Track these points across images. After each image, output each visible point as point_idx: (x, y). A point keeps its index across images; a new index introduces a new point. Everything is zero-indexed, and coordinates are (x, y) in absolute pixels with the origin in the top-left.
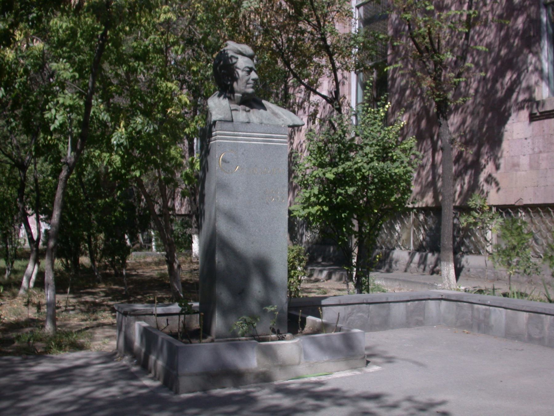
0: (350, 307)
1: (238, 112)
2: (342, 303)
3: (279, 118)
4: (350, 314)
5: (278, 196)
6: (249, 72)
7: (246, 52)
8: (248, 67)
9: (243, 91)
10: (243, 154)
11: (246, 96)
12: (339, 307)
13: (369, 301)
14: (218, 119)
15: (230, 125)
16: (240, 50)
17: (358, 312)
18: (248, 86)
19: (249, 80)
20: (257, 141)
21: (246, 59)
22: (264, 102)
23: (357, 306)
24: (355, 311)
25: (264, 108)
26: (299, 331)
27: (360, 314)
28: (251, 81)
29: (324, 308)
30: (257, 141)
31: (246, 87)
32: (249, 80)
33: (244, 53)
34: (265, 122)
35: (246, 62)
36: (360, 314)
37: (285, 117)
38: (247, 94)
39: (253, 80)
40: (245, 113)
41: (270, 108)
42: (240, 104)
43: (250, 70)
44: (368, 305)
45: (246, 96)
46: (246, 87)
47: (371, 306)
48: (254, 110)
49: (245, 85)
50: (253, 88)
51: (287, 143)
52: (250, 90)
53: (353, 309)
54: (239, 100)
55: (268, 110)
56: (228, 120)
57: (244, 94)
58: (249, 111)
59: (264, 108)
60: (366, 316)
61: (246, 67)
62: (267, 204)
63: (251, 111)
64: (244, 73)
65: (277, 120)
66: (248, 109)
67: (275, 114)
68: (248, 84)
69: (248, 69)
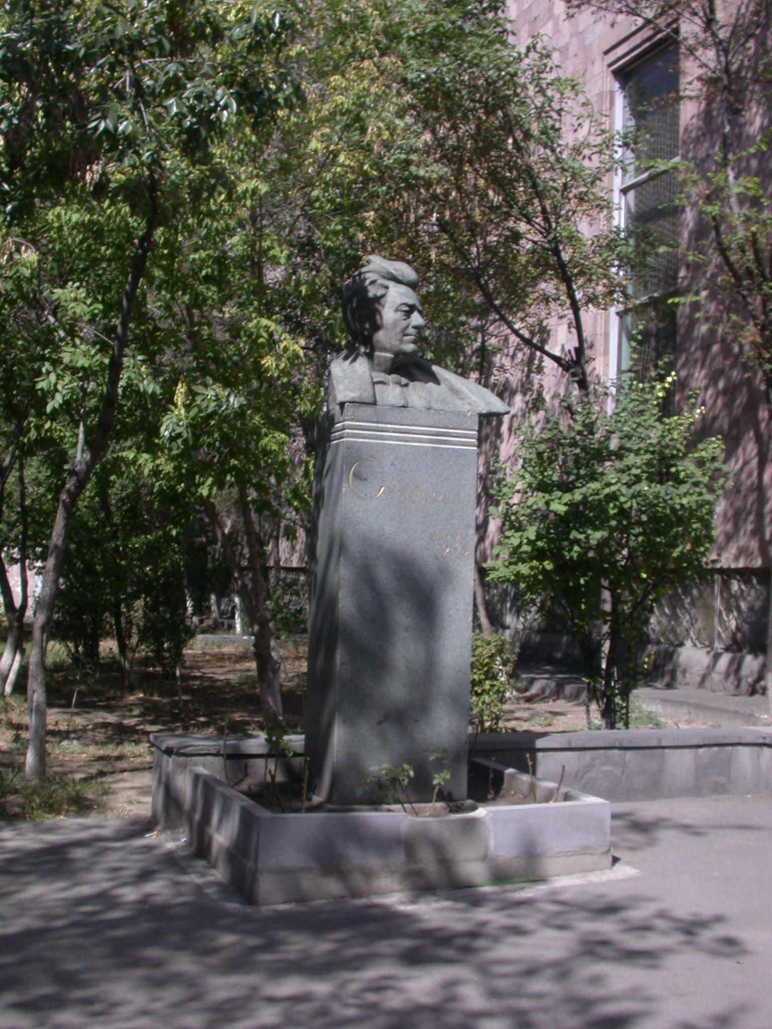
0: (588, 754)
1: (385, 387)
2: (573, 746)
3: (462, 399)
4: (589, 767)
6: (408, 314)
7: (403, 276)
10: (392, 464)
11: (401, 357)
12: (568, 753)
13: (625, 744)
14: (347, 399)
15: (369, 410)
16: (393, 272)
17: (603, 764)
18: (406, 338)
19: (407, 327)
20: (420, 441)
21: (403, 289)
22: (435, 368)
23: (602, 751)
24: (597, 762)
25: (434, 379)
26: (490, 797)
27: (607, 768)
28: (411, 330)
29: (540, 755)
30: (420, 441)
31: (401, 341)
32: (407, 327)
34: (436, 406)
35: (402, 295)
36: (607, 768)
37: (473, 398)
38: (405, 353)
39: (415, 327)
40: (398, 389)
41: (446, 380)
42: (390, 372)
43: (411, 309)
44: (622, 752)
45: (401, 357)
46: (401, 341)
47: (629, 754)
49: (399, 337)
50: (414, 342)
52: (410, 347)
53: (593, 759)
54: (389, 364)
55: (443, 385)
57: (398, 354)
58: (406, 385)
59: (434, 379)
60: (618, 772)
63: (411, 384)
64: (399, 315)
65: (459, 402)
66: (404, 381)
67: (454, 391)
69: (406, 309)
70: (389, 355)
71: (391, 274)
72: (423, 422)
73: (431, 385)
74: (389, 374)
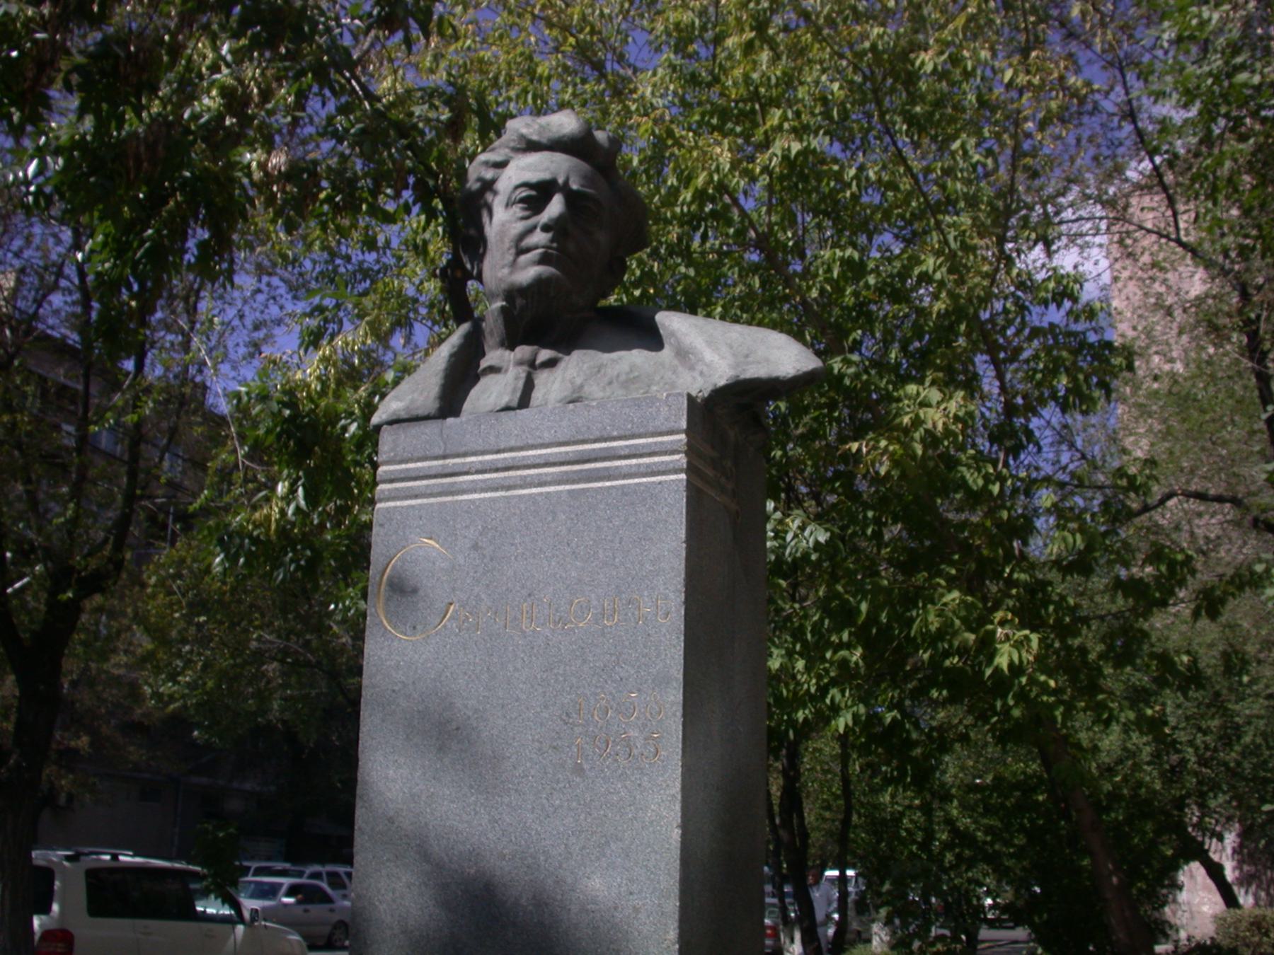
3: (692, 368)
5: (634, 733)
8: (526, 185)
9: (503, 286)
10: (475, 547)
11: (519, 302)
16: (524, 131)
28: (539, 237)
33: (535, 138)
41: (673, 334)
48: (577, 354)
50: (543, 260)
51: (676, 471)
55: (666, 353)
56: (421, 412)
58: (551, 364)
61: (517, 187)
62: (579, 770)
64: (517, 210)
66: (545, 354)
67: (683, 354)
68: (521, 251)
70: (499, 303)
71: (522, 137)
72: (547, 437)
73: (637, 358)
74: (512, 348)
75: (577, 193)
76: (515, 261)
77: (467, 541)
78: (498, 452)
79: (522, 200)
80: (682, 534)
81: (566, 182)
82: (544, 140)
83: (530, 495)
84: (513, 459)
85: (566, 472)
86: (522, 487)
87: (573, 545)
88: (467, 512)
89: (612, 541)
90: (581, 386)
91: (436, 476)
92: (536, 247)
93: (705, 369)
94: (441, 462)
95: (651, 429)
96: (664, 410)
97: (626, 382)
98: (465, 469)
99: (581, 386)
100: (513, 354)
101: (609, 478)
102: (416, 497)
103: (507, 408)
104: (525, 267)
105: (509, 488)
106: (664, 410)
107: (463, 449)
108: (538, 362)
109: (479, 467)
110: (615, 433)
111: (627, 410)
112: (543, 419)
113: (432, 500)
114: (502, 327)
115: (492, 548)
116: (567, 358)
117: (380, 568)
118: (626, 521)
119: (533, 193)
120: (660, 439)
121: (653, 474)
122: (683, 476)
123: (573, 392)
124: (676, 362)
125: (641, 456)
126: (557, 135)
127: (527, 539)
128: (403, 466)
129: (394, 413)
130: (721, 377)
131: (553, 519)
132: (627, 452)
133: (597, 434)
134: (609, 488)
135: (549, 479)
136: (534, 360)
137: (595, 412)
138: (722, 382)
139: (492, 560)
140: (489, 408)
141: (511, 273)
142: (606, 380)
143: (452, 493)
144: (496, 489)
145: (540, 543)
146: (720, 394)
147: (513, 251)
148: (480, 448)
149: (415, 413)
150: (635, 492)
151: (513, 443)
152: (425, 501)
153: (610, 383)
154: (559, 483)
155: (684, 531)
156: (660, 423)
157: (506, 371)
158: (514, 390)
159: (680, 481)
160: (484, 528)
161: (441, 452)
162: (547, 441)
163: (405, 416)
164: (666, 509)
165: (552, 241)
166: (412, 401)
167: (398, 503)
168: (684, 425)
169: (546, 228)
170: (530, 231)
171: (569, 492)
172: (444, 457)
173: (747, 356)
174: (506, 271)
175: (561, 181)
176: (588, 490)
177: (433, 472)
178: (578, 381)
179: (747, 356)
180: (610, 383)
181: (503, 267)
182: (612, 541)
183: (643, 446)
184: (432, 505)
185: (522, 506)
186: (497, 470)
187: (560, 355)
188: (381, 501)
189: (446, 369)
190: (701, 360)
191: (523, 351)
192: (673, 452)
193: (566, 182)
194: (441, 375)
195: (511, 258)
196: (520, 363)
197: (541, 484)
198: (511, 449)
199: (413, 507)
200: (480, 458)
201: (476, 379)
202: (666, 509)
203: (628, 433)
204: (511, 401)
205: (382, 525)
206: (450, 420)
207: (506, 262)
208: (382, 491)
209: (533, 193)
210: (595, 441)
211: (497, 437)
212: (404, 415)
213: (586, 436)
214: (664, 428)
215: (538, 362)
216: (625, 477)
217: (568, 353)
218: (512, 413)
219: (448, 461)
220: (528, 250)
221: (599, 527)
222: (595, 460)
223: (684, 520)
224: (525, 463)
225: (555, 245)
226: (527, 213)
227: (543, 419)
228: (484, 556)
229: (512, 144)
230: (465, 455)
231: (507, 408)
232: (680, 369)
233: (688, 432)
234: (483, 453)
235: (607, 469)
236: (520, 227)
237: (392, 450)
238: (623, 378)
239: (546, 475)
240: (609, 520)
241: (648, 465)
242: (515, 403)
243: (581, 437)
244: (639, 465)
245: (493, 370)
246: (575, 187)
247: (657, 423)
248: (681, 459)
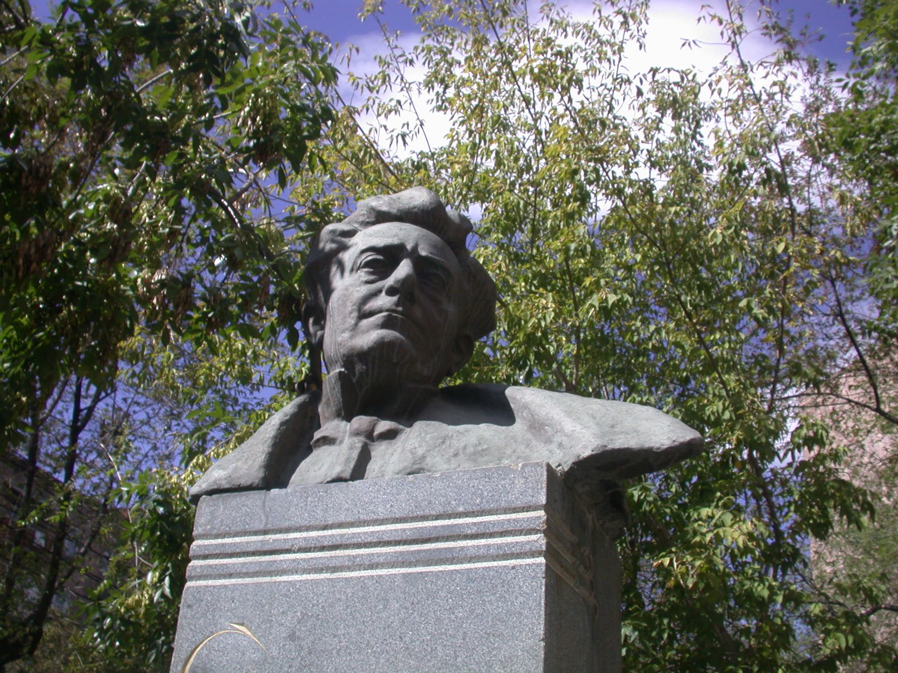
3: (549, 441)
9: (343, 351)
10: (292, 637)
11: (359, 367)
28: (384, 301)
33: (385, 208)
38: (363, 356)
41: (525, 407)
48: (419, 425)
50: (387, 324)
51: (533, 554)
55: (518, 427)
56: (244, 482)
58: (390, 435)
66: (384, 426)
67: (538, 427)
68: (364, 315)
70: (338, 369)
74: (348, 419)
75: (425, 259)
76: (356, 324)
77: (283, 629)
78: (325, 528)
79: (367, 264)
80: (541, 630)
81: (415, 248)
82: (394, 211)
83: (359, 578)
84: (342, 536)
85: (402, 553)
86: (349, 569)
87: (407, 639)
88: (286, 595)
89: (454, 637)
90: (423, 457)
91: (254, 554)
92: (380, 311)
93: (565, 440)
94: (260, 538)
95: (503, 504)
96: (520, 483)
97: (474, 453)
98: (287, 547)
99: (423, 457)
100: (349, 424)
101: (452, 561)
102: (231, 576)
103: (339, 479)
104: (368, 330)
105: (335, 569)
106: (520, 483)
107: (286, 524)
108: (376, 433)
109: (303, 544)
110: (461, 509)
111: (476, 482)
112: (378, 491)
113: (248, 580)
114: (339, 395)
115: (311, 638)
116: (408, 430)
117: (184, 656)
118: (472, 611)
119: (380, 257)
120: (513, 516)
121: (506, 557)
122: (542, 560)
123: (414, 463)
124: (529, 436)
125: (492, 535)
126: (407, 207)
127: (352, 630)
128: (220, 541)
129: (215, 482)
130: (585, 447)
131: (385, 607)
132: (474, 530)
133: (440, 509)
134: (452, 572)
135: (382, 560)
136: (373, 431)
137: (438, 485)
138: (587, 453)
139: (310, 653)
140: (319, 480)
141: (351, 337)
142: (451, 451)
143: (270, 573)
144: (320, 571)
145: (367, 636)
146: (583, 467)
147: (355, 314)
148: (306, 523)
149: (237, 482)
150: (483, 578)
151: (342, 518)
152: (240, 581)
153: (456, 455)
154: (393, 565)
155: (542, 627)
156: (515, 498)
157: (341, 442)
158: (348, 460)
159: (538, 565)
160: (304, 615)
161: (262, 527)
162: (381, 516)
163: (227, 486)
164: (521, 599)
165: (397, 304)
166: (236, 469)
167: (211, 582)
168: (543, 500)
169: (391, 291)
170: (375, 294)
171: (404, 575)
172: (265, 532)
173: (613, 426)
174: (346, 335)
175: (409, 247)
176: (427, 573)
177: (251, 549)
178: (420, 452)
179: (613, 426)
180: (456, 455)
181: (343, 331)
182: (454, 637)
183: (494, 524)
184: (247, 585)
185: (349, 590)
186: (323, 548)
187: (401, 427)
188: (192, 578)
189: (275, 437)
190: (561, 431)
191: (361, 421)
192: (530, 532)
193: (415, 248)
194: (269, 442)
195: (353, 322)
196: (357, 433)
197: (372, 567)
198: (340, 525)
199: (226, 587)
200: (305, 534)
201: (309, 450)
202: (521, 599)
203: (475, 508)
204: (342, 472)
205: (189, 606)
206: (275, 491)
207: (347, 326)
208: (194, 568)
209: (380, 257)
210: (437, 517)
211: (325, 511)
212: (225, 485)
213: (427, 512)
214: (519, 503)
215: (376, 433)
216: (471, 560)
217: (410, 425)
218: (344, 484)
219: (268, 537)
220: (371, 314)
221: (438, 619)
222: (437, 539)
223: (543, 613)
224: (355, 541)
225: (400, 309)
226: (372, 277)
227: (378, 491)
228: (302, 648)
229: (361, 219)
230: (288, 530)
231: (339, 479)
232: (534, 442)
233: (547, 508)
234: (308, 528)
235: (450, 550)
236: (365, 290)
237: (210, 522)
238: (470, 450)
239: (379, 555)
240: (451, 611)
241: (499, 547)
242: (347, 474)
243: (421, 513)
244: (489, 546)
245: (327, 441)
246: (423, 253)
247: (511, 497)
248: (539, 540)
